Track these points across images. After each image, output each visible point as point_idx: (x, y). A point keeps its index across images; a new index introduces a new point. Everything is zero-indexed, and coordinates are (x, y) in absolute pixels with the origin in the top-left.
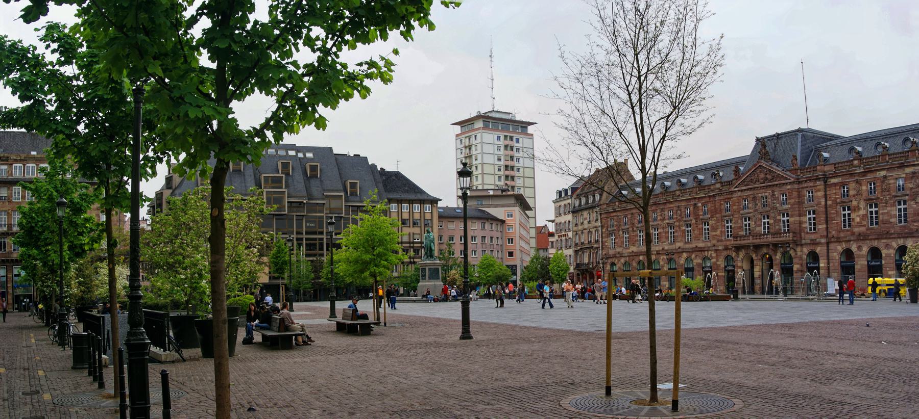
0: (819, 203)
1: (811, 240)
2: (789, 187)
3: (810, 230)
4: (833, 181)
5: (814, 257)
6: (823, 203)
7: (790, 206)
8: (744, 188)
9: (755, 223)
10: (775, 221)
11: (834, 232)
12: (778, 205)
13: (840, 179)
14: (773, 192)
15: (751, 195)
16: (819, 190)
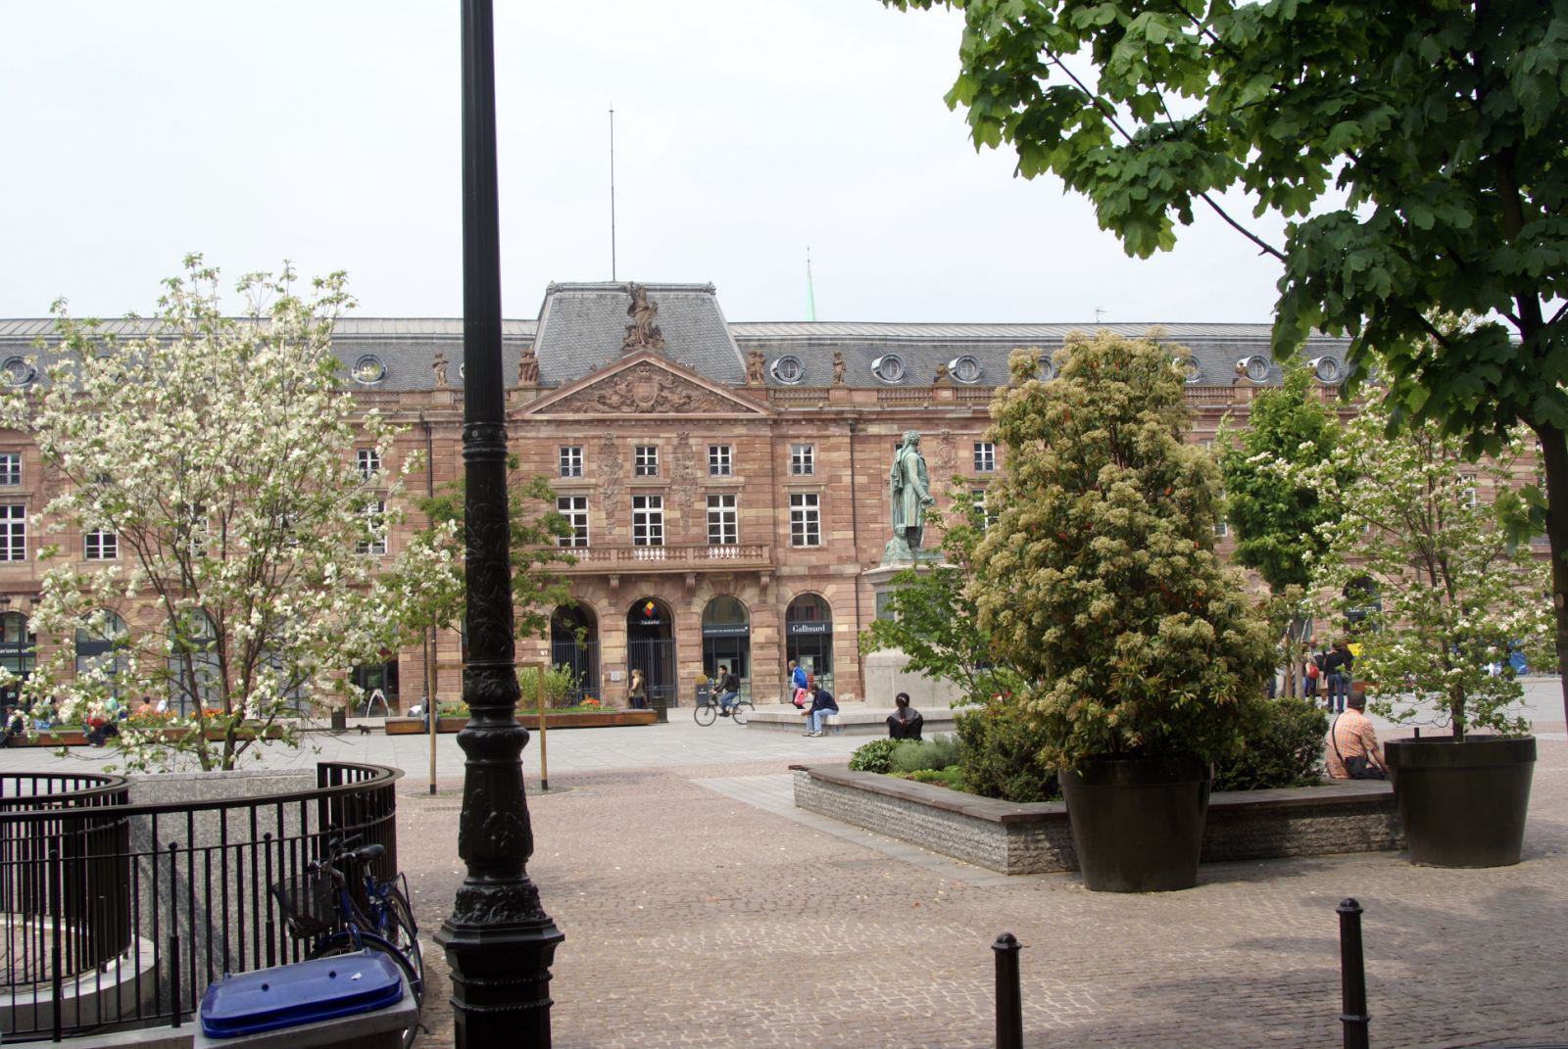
0: (834, 479)
1: (810, 568)
2: (740, 430)
3: (798, 541)
4: (874, 429)
5: (812, 607)
6: (847, 479)
7: (742, 479)
8: (570, 416)
9: (610, 515)
10: (685, 515)
11: (874, 551)
12: (699, 474)
13: (895, 427)
14: (684, 438)
15: (593, 438)
16: (836, 448)
